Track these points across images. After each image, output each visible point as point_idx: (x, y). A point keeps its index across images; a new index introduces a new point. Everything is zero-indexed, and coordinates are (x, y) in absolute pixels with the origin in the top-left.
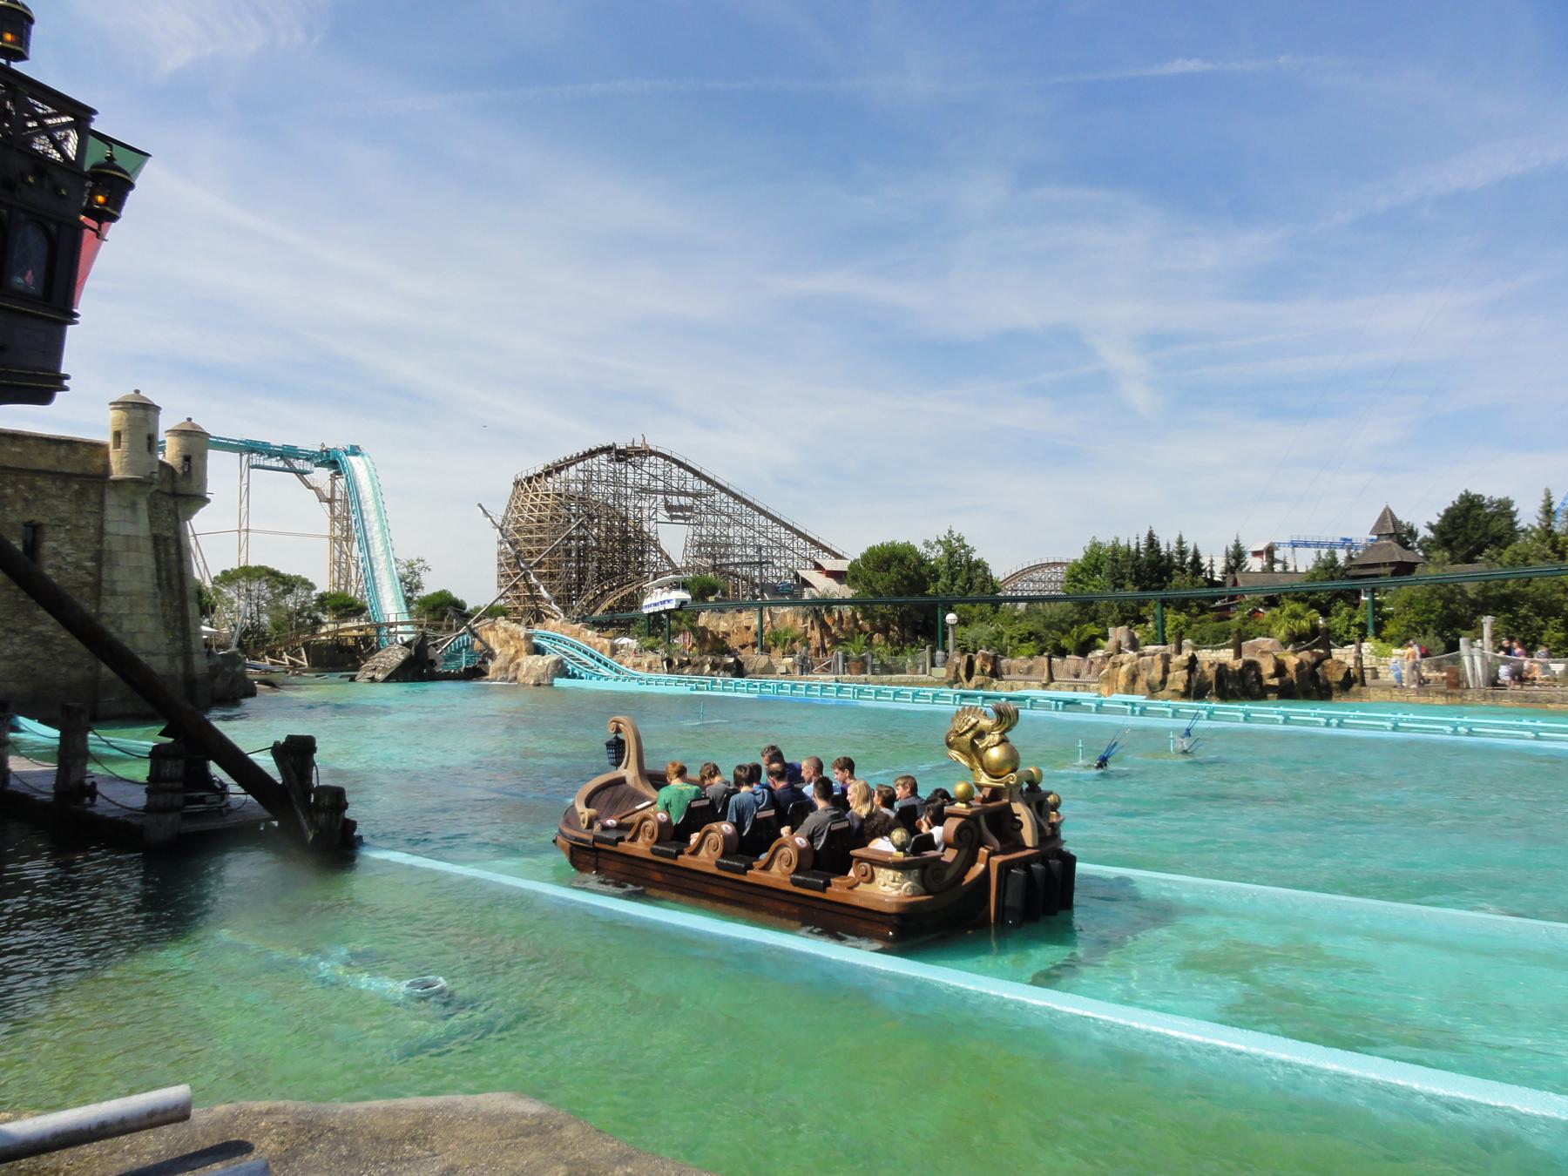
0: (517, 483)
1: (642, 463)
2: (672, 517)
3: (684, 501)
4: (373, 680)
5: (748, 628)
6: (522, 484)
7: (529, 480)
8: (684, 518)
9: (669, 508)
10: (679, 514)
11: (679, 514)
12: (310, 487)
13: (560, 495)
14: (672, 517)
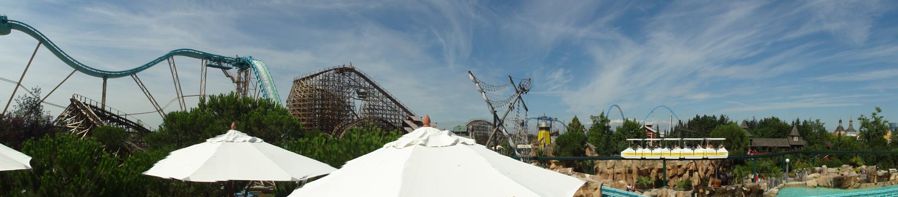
2: (360, 97)
3: (362, 90)
5: (679, 167)
6: (300, 81)
7: (303, 79)
9: (358, 93)
12: (228, 76)
14: (360, 97)
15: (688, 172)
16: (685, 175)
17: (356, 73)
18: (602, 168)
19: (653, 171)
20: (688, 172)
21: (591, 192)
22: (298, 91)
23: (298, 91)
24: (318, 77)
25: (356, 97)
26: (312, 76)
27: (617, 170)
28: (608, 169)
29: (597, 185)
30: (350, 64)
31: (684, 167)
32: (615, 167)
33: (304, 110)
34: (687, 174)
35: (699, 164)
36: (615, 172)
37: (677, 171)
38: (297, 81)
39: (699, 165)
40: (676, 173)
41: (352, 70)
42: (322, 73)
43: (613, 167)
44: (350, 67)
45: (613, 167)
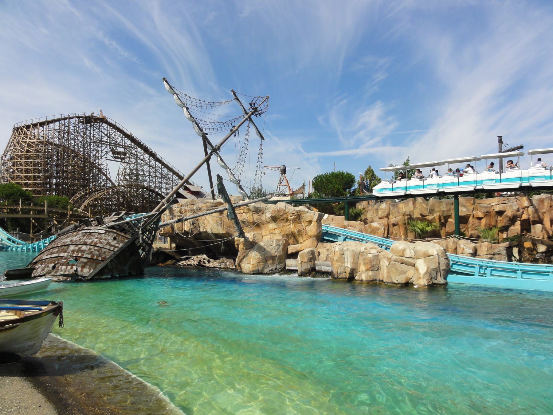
0: (16, 129)
1: (100, 126)
2: (116, 158)
3: (120, 149)
4: (75, 278)
5: (500, 213)
6: (22, 129)
7: (28, 127)
8: (122, 159)
9: (114, 152)
10: (119, 156)
11: (119, 156)
13: (48, 137)
15: (518, 223)
16: (512, 228)
17: (111, 126)
18: (371, 218)
19: (450, 220)
20: (518, 223)
21: (304, 227)
22: (18, 143)
23: (18, 143)
24: (51, 125)
25: (109, 158)
26: (42, 124)
27: (393, 220)
28: (380, 218)
29: (311, 217)
30: (99, 113)
31: (509, 213)
32: (391, 216)
33: (27, 171)
34: (516, 228)
35: (544, 210)
36: (390, 224)
37: (497, 221)
38: (18, 129)
39: (543, 213)
40: (493, 223)
41: (103, 120)
42: (58, 120)
43: (387, 216)
44: (101, 117)
45: (387, 216)
